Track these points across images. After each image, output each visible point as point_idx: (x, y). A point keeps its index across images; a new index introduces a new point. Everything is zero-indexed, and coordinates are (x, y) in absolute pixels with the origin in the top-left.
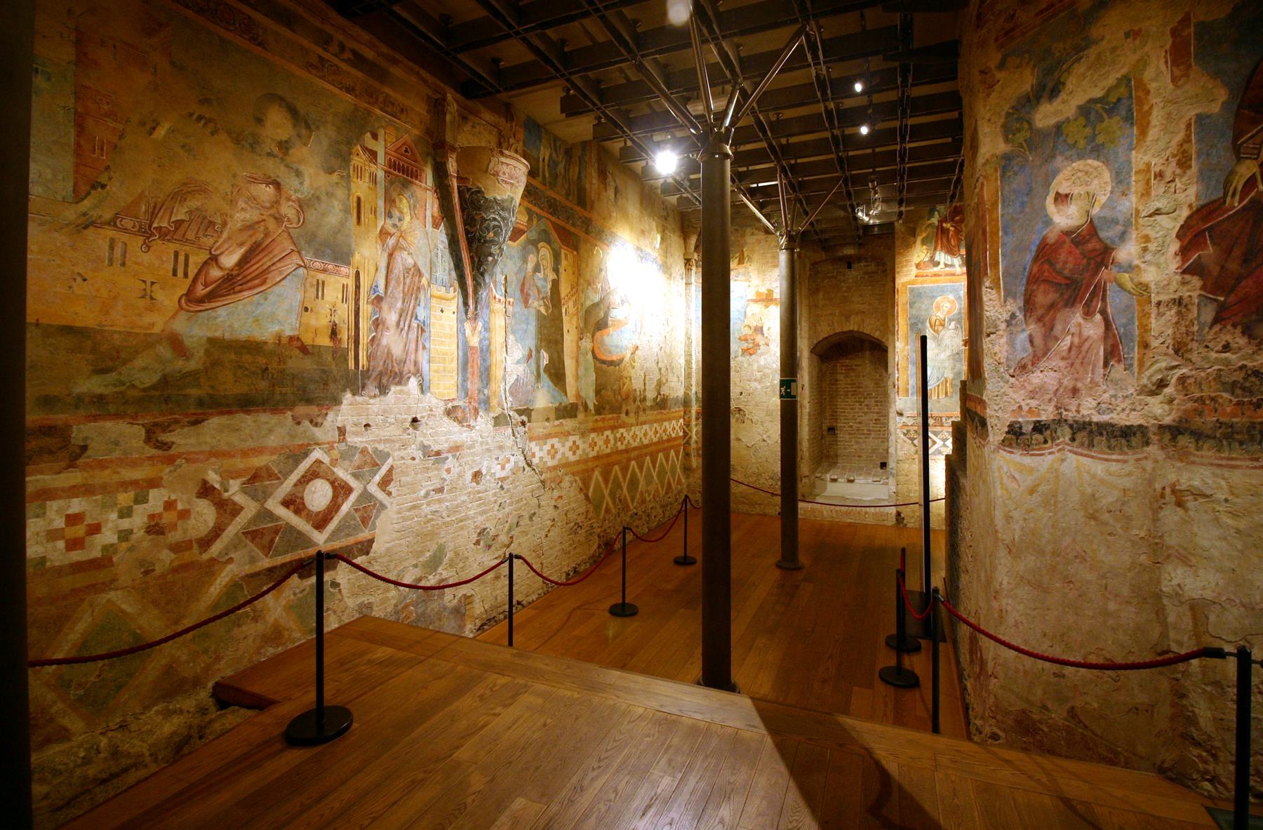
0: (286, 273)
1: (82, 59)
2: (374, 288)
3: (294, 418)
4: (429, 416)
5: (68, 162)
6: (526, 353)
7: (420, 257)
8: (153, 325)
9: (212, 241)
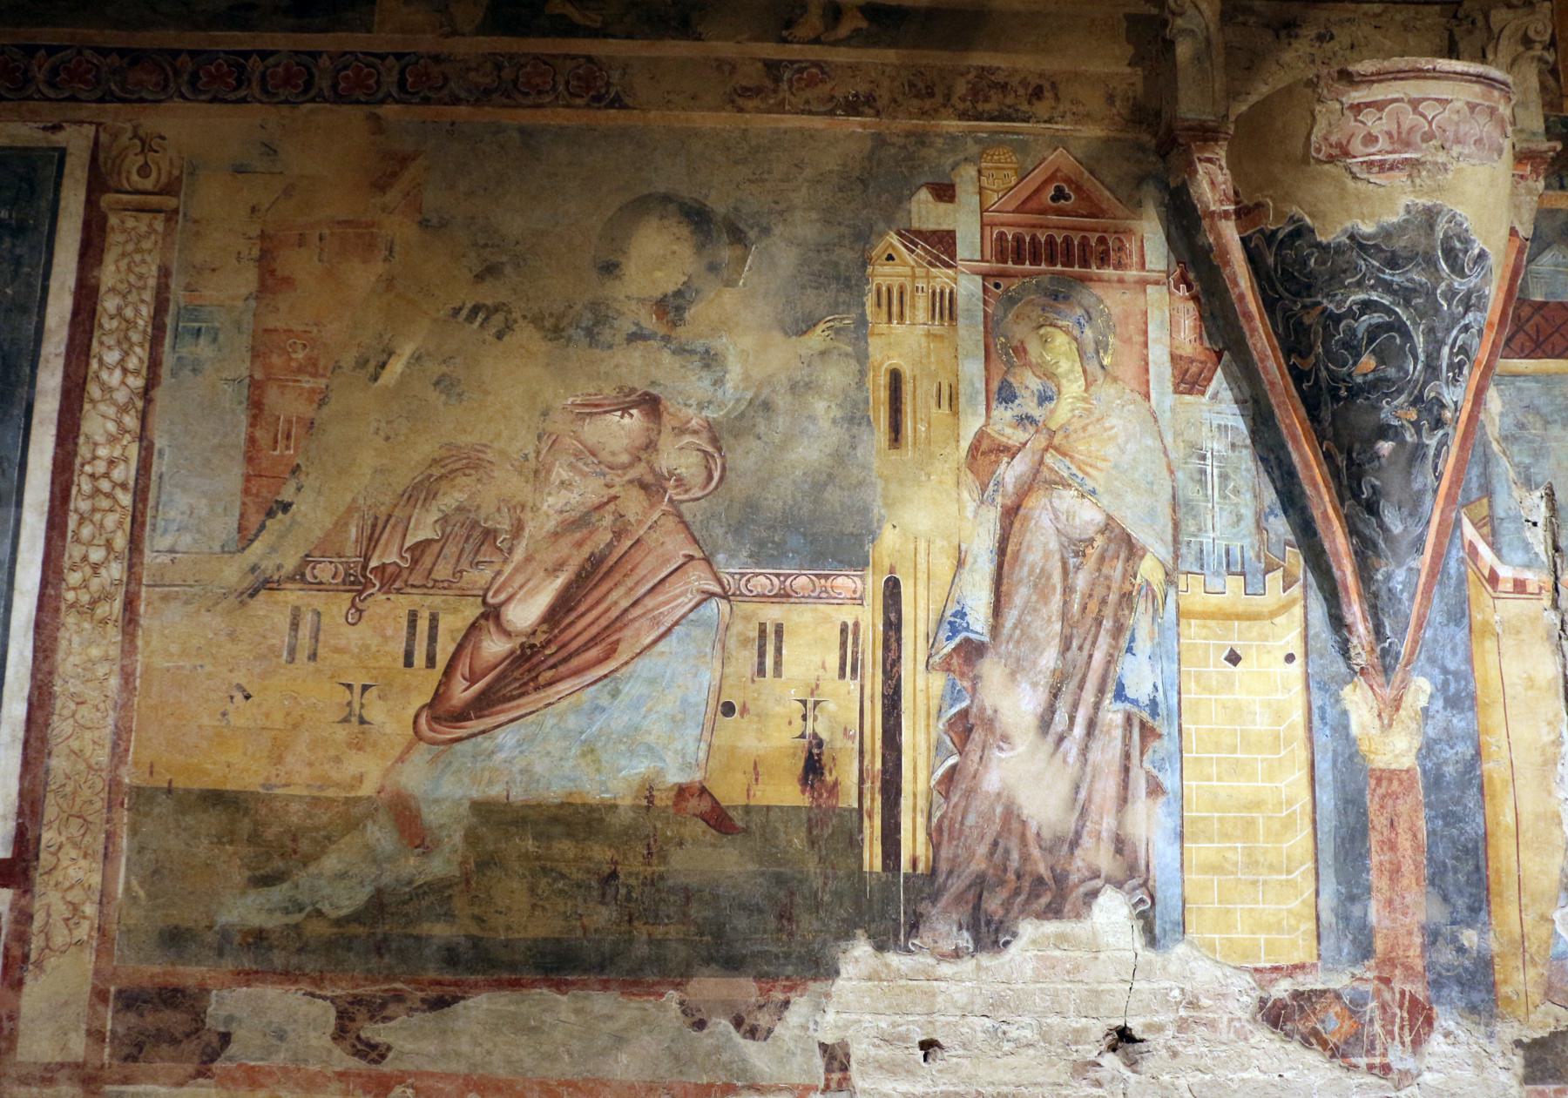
1: (271, 281)
3: (685, 1008)
4: (1182, 1026)
5: (232, 477)
7: (1130, 498)
8: (360, 778)
9: (488, 573)
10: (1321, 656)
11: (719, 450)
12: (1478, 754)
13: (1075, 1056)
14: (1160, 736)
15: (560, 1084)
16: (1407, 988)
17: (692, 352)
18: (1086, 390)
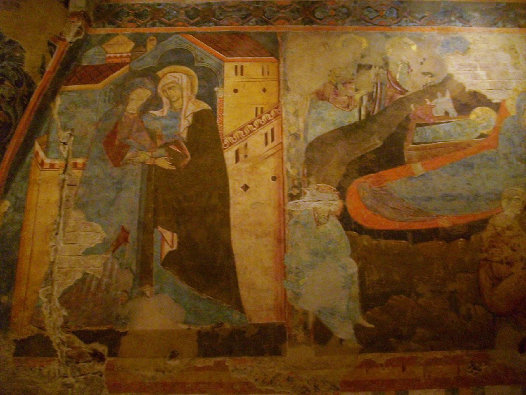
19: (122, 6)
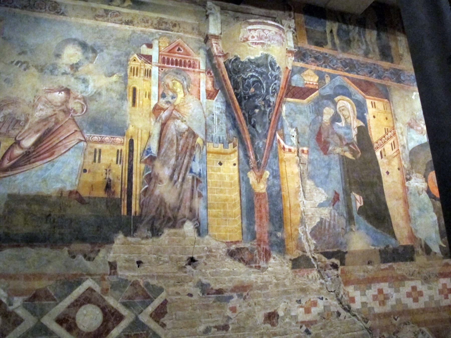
0: (69, 147)
2: (147, 151)
3: (69, 252)
6: (331, 195)
9: (17, 132)
10: (243, 164)
11: (86, 104)
12: (280, 190)
13: (179, 265)
14: (201, 182)
15: (30, 275)
16: (264, 247)
17: (80, 79)
18: (184, 96)
19: (306, 50)
